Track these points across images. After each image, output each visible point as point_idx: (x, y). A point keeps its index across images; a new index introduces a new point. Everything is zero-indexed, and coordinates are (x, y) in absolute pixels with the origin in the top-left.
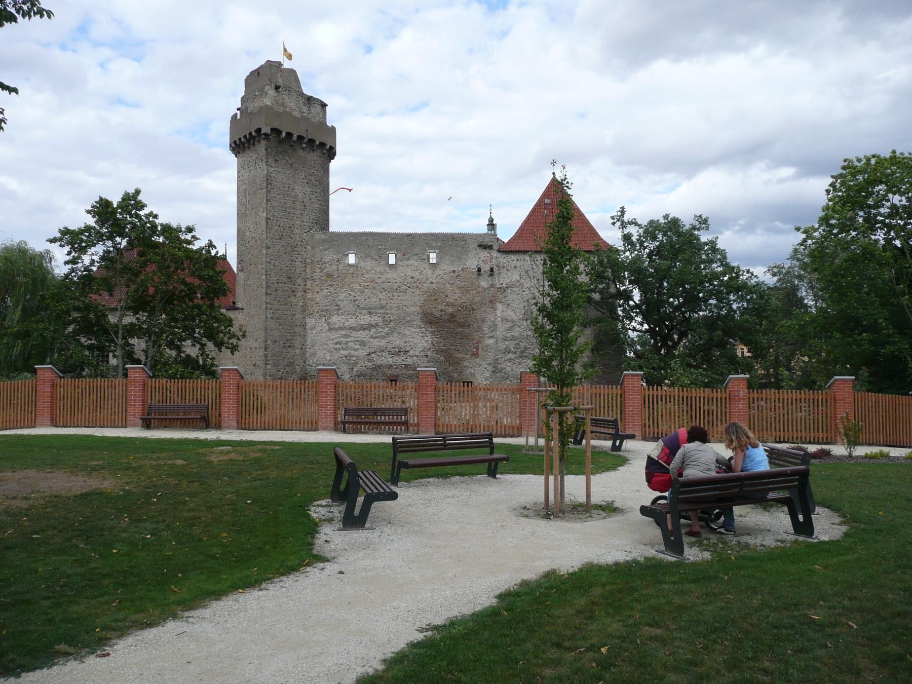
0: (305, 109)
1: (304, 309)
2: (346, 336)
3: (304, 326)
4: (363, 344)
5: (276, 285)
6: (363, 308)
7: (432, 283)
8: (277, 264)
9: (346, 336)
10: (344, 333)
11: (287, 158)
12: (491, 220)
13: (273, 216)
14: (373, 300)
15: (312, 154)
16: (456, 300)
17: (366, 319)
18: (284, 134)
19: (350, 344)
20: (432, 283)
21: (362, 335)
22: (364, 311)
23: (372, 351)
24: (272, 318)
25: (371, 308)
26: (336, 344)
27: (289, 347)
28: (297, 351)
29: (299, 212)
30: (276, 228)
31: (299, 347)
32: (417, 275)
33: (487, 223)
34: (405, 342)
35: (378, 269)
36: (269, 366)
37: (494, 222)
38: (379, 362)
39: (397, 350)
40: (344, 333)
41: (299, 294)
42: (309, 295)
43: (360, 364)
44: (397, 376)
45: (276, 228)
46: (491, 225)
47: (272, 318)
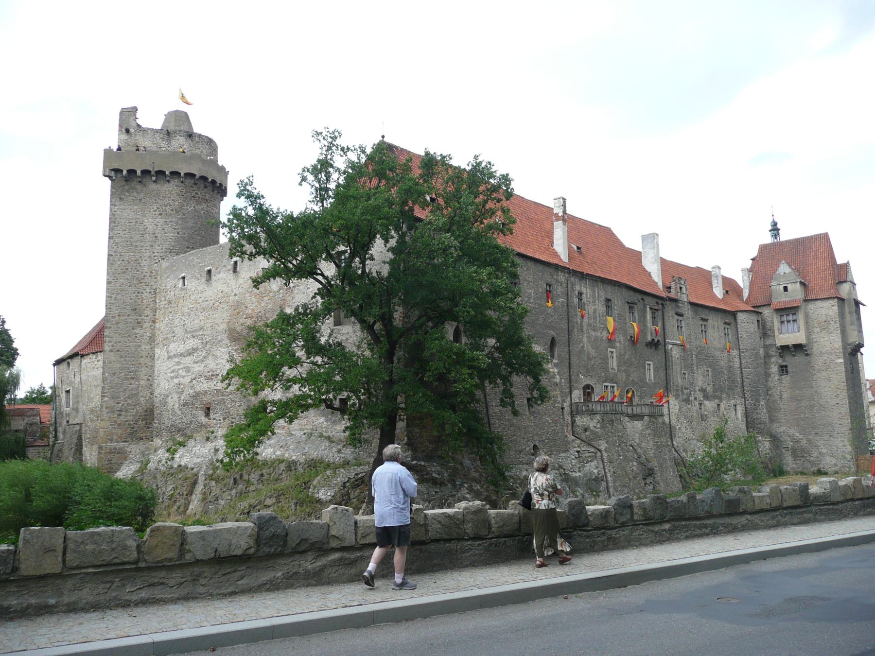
0: (164, 144)
1: (152, 339)
2: (178, 363)
3: (152, 357)
4: (188, 370)
5: (117, 318)
6: (189, 332)
7: (235, 295)
8: (119, 297)
9: (178, 363)
10: (177, 360)
11: (135, 194)
12: (775, 224)
13: (116, 252)
14: (196, 322)
15: (167, 185)
16: (253, 310)
17: (191, 343)
18: (125, 172)
19: (180, 371)
20: (235, 295)
21: (188, 360)
22: (189, 335)
23: (193, 377)
24: (111, 351)
25: (194, 331)
26: (173, 371)
27: (132, 378)
28: (143, 383)
29: (148, 244)
30: (119, 263)
31: (145, 378)
32: (226, 290)
33: (770, 228)
34: (217, 365)
35: (199, 288)
36: (106, 399)
37: (779, 226)
38: (198, 389)
39: (210, 374)
40: (177, 360)
41: (146, 325)
42: (157, 325)
43: (186, 392)
44: (210, 403)
45: (119, 263)
46: (775, 229)
47: (111, 351)
